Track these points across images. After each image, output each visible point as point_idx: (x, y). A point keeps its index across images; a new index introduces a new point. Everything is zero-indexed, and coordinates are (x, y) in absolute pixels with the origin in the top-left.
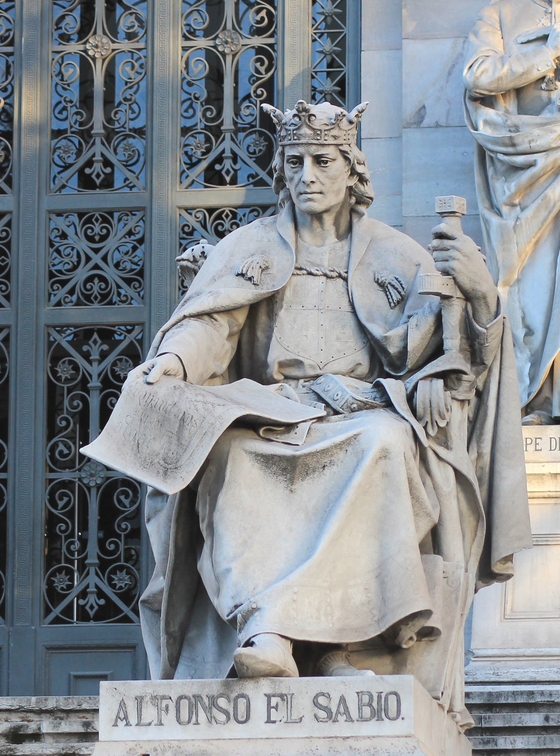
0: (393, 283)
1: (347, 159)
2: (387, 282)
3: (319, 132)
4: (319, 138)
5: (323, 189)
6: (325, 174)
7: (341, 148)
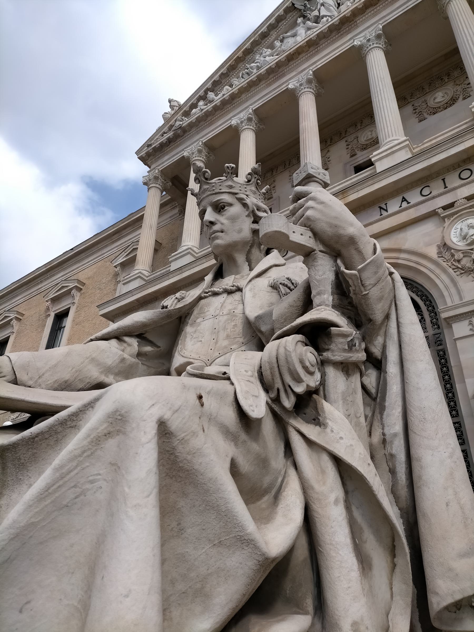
0: (286, 283)
1: (245, 205)
2: (279, 283)
3: (214, 185)
4: (214, 188)
5: (224, 228)
6: (224, 217)
7: (237, 196)
